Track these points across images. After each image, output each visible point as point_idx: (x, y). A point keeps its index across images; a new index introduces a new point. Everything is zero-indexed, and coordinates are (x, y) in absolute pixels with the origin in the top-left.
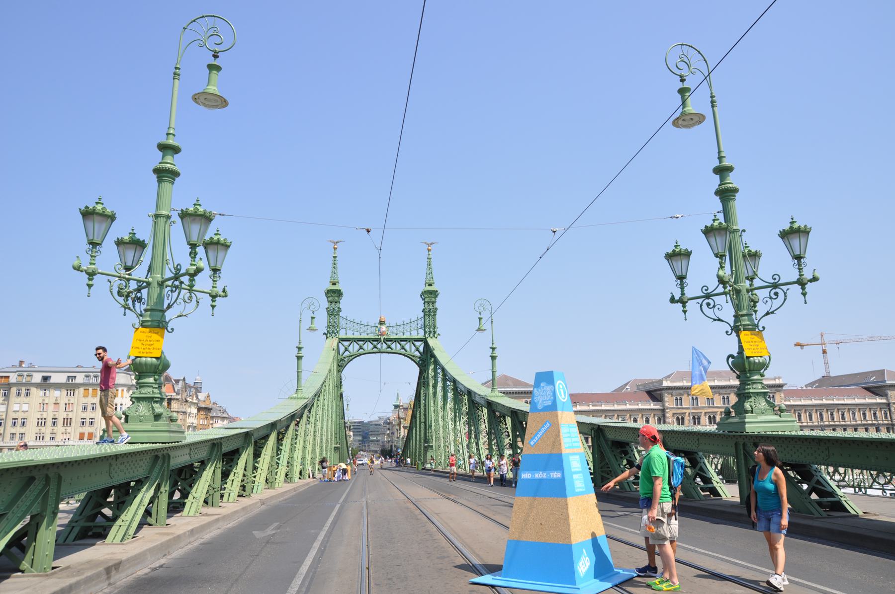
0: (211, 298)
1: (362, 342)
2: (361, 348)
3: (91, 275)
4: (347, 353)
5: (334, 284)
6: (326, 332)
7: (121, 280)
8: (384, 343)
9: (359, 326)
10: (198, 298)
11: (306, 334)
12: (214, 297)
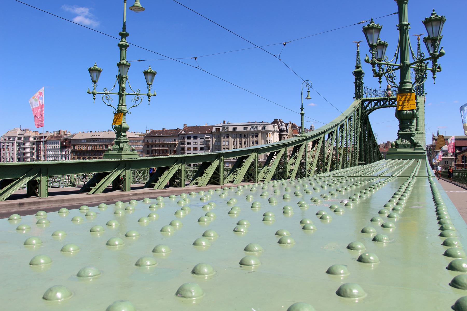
0: (148, 97)
1: (376, 101)
2: (375, 105)
3: (94, 94)
4: (368, 108)
5: (358, 68)
6: (355, 97)
7: (106, 95)
8: (390, 101)
9: (374, 92)
10: (142, 98)
11: (305, 101)
12: (149, 96)
